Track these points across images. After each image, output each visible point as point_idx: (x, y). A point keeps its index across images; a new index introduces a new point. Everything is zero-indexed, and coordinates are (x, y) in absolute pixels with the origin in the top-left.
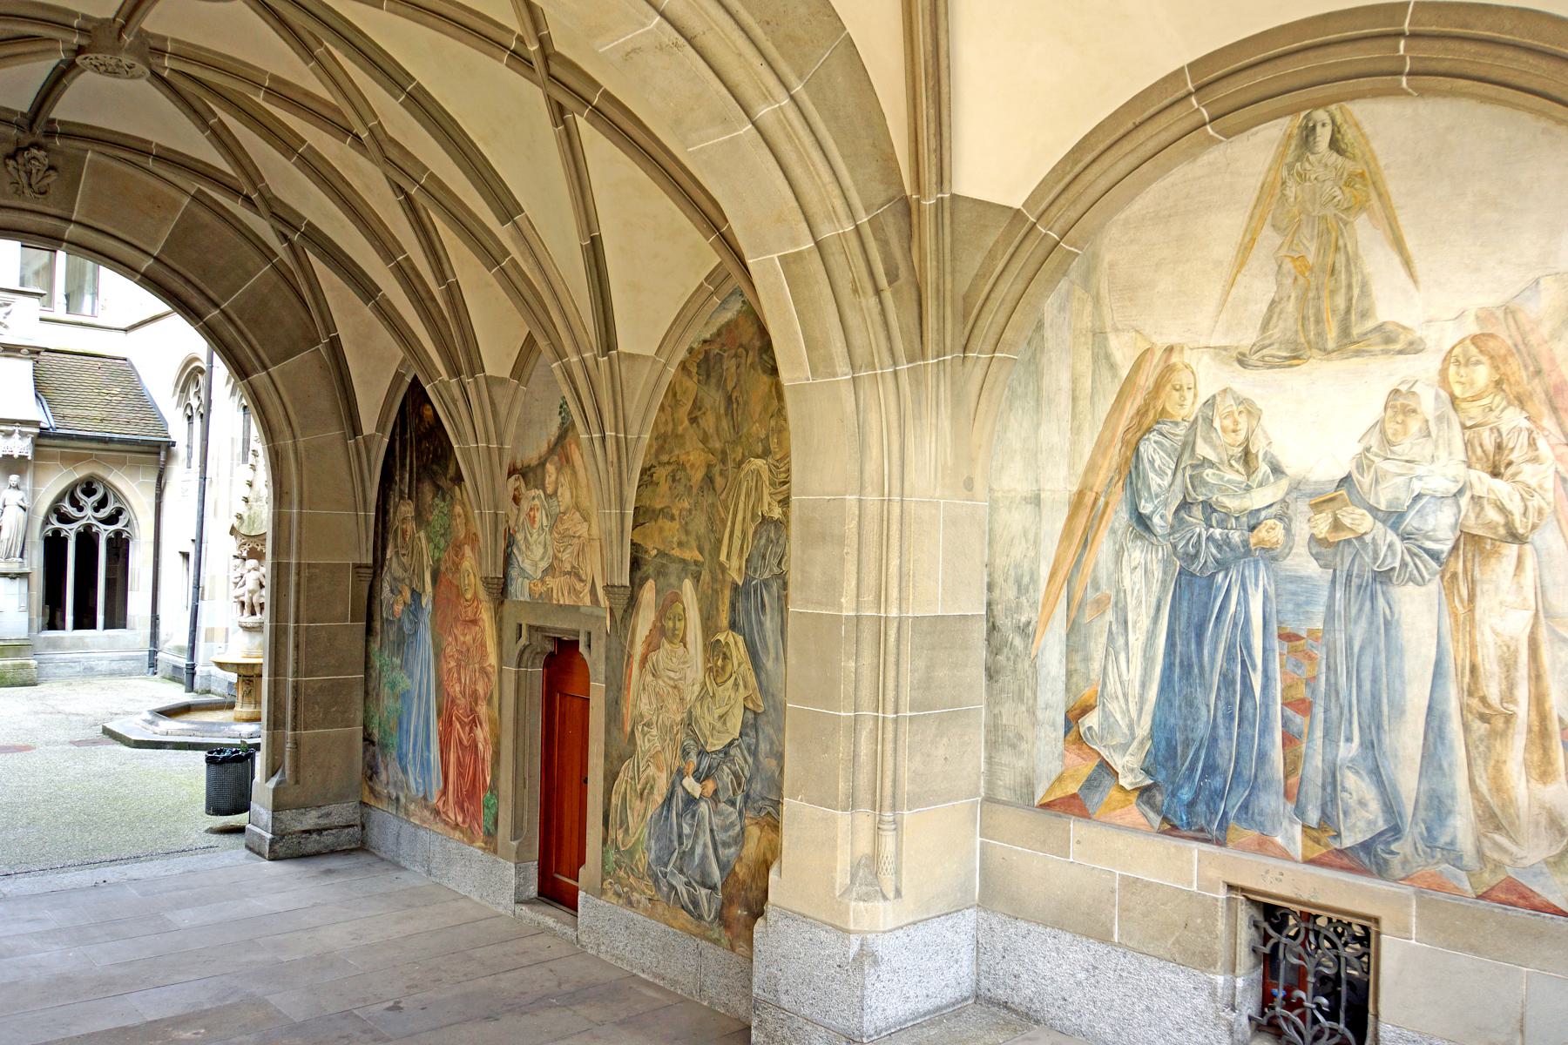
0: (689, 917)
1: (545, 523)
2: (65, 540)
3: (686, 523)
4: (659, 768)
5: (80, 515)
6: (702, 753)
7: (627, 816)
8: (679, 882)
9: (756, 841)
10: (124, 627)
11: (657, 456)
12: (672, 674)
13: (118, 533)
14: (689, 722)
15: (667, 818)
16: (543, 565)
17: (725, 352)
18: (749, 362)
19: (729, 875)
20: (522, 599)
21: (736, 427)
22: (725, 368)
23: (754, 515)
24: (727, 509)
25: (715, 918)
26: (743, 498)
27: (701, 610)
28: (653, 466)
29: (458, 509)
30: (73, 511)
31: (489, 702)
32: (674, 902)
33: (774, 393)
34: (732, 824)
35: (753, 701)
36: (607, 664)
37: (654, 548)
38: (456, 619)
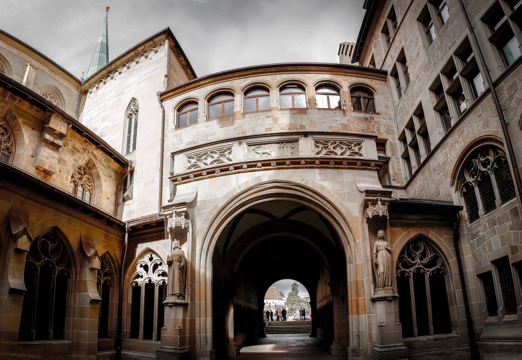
2: (408, 278)
5: (414, 262)
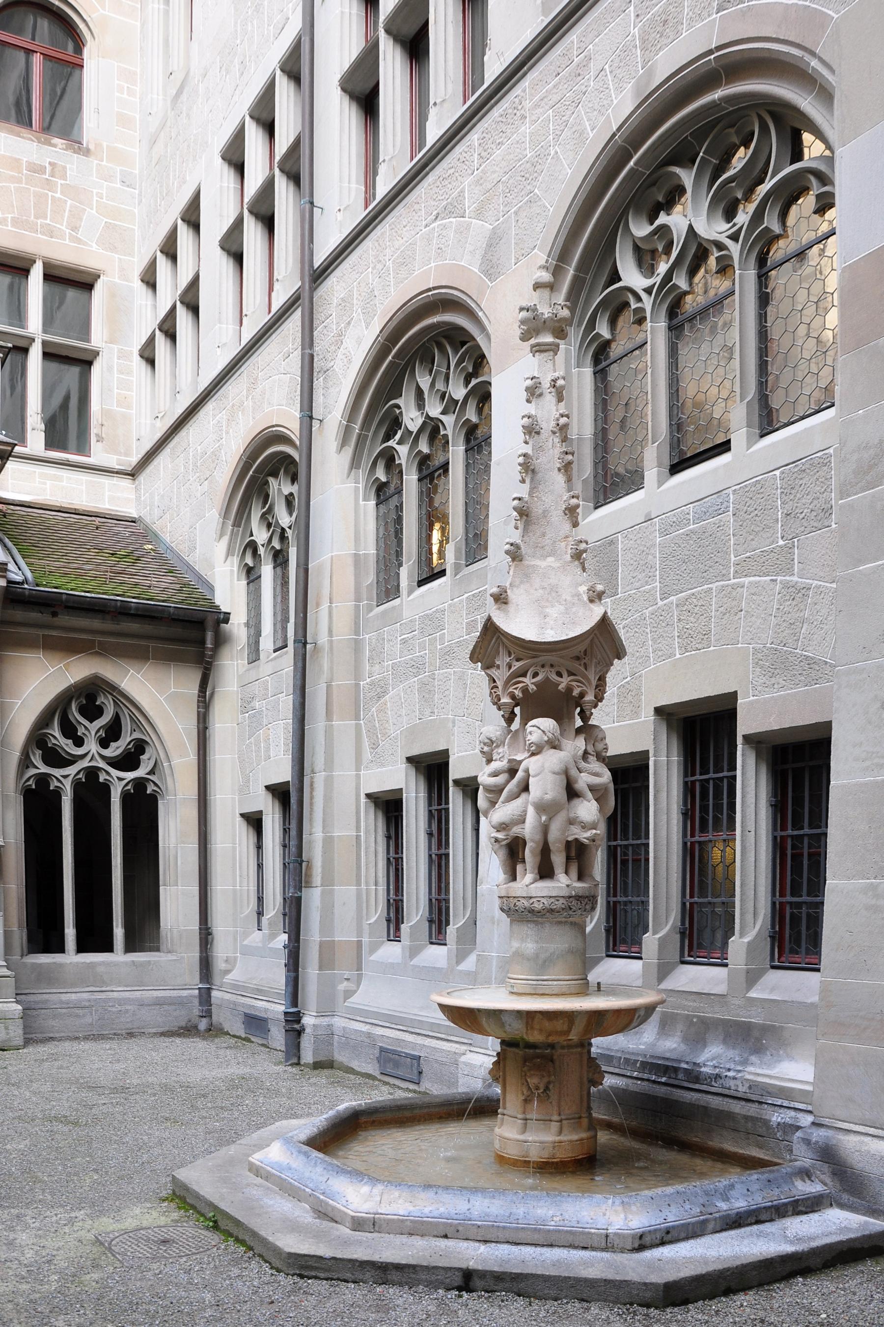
2: (57, 795)
5: (79, 751)
10: (158, 950)
13: (140, 784)
30: (67, 745)
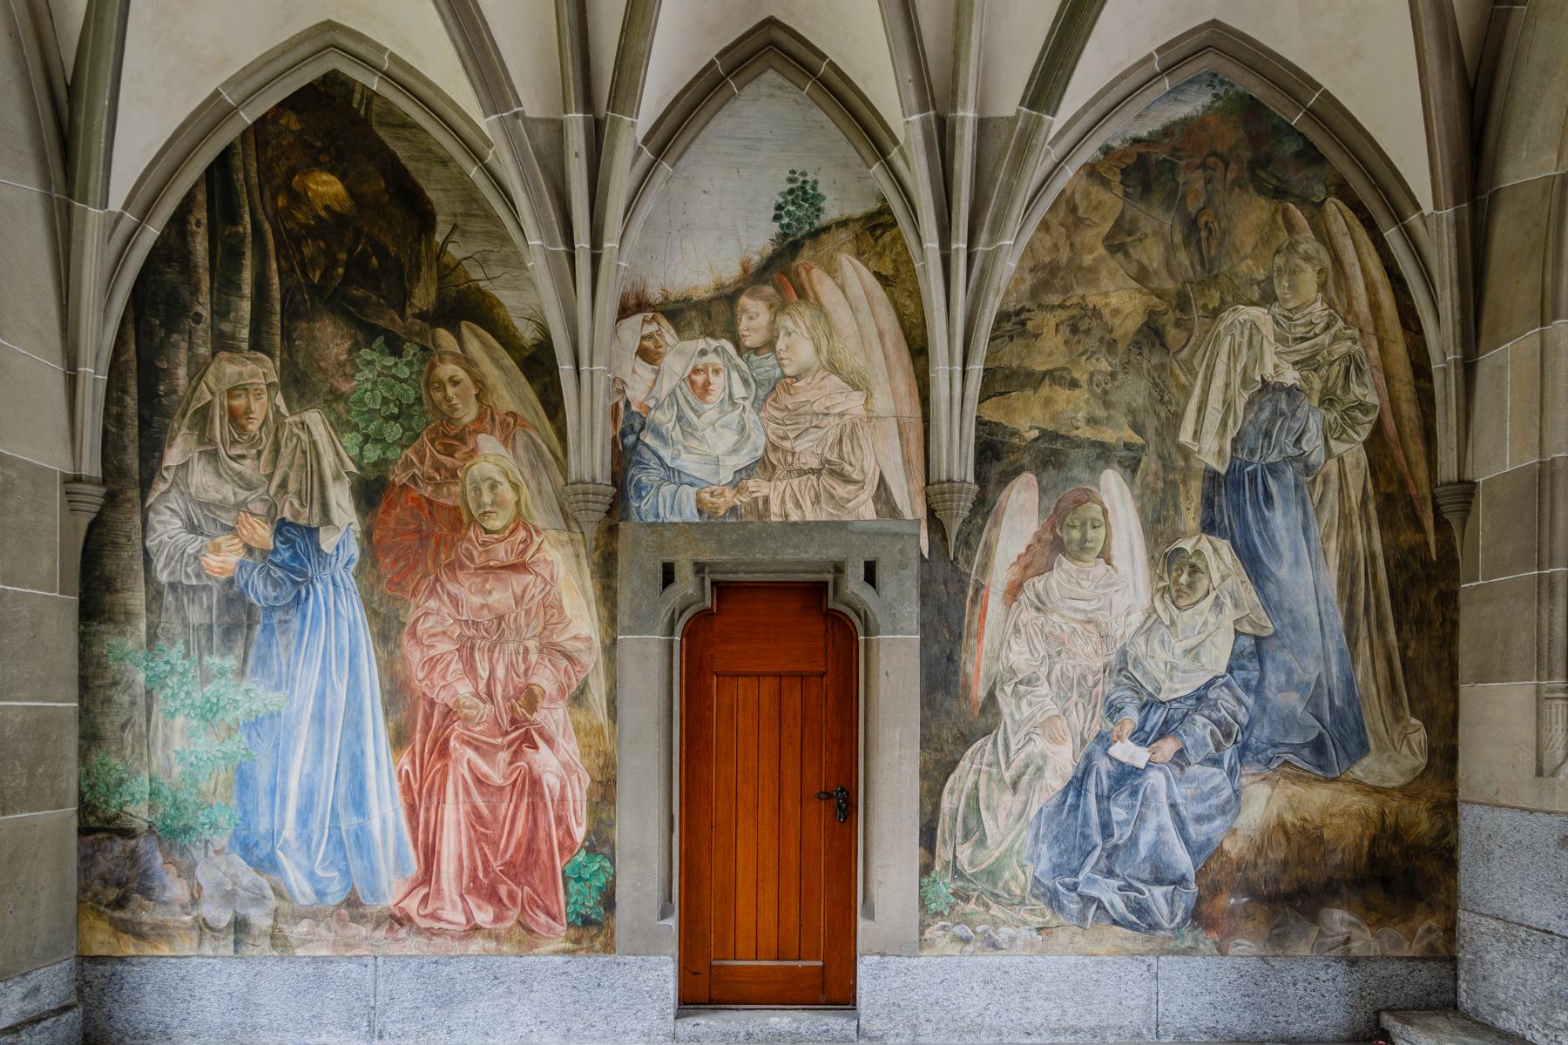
0: (1129, 932)
1: (739, 390)
3: (1105, 392)
4: (1053, 740)
6: (1148, 706)
7: (980, 821)
8: (1109, 893)
9: (1264, 801)
11: (1034, 293)
12: (1081, 605)
14: (1122, 667)
15: (1075, 807)
16: (743, 460)
17: (1181, 158)
18: (1230, 176)
19: (1211, 857)
20: (676, 519)
21: (1207, 264)
22: (1181, 180)
23: (1246, 382)
24: (1192, 372)
25: (1184, 921)
26: (1223, 357)
27: (1141, 511)
28: (1022, 310)
29: (448, 370)
31: (579, 698)
32: (1096, 920)
33: (1280, 219)
34: (1216, 790)
35: (1252, 623)
36: (923, 604)
37: (1031, 428)
38: (454, 567)
